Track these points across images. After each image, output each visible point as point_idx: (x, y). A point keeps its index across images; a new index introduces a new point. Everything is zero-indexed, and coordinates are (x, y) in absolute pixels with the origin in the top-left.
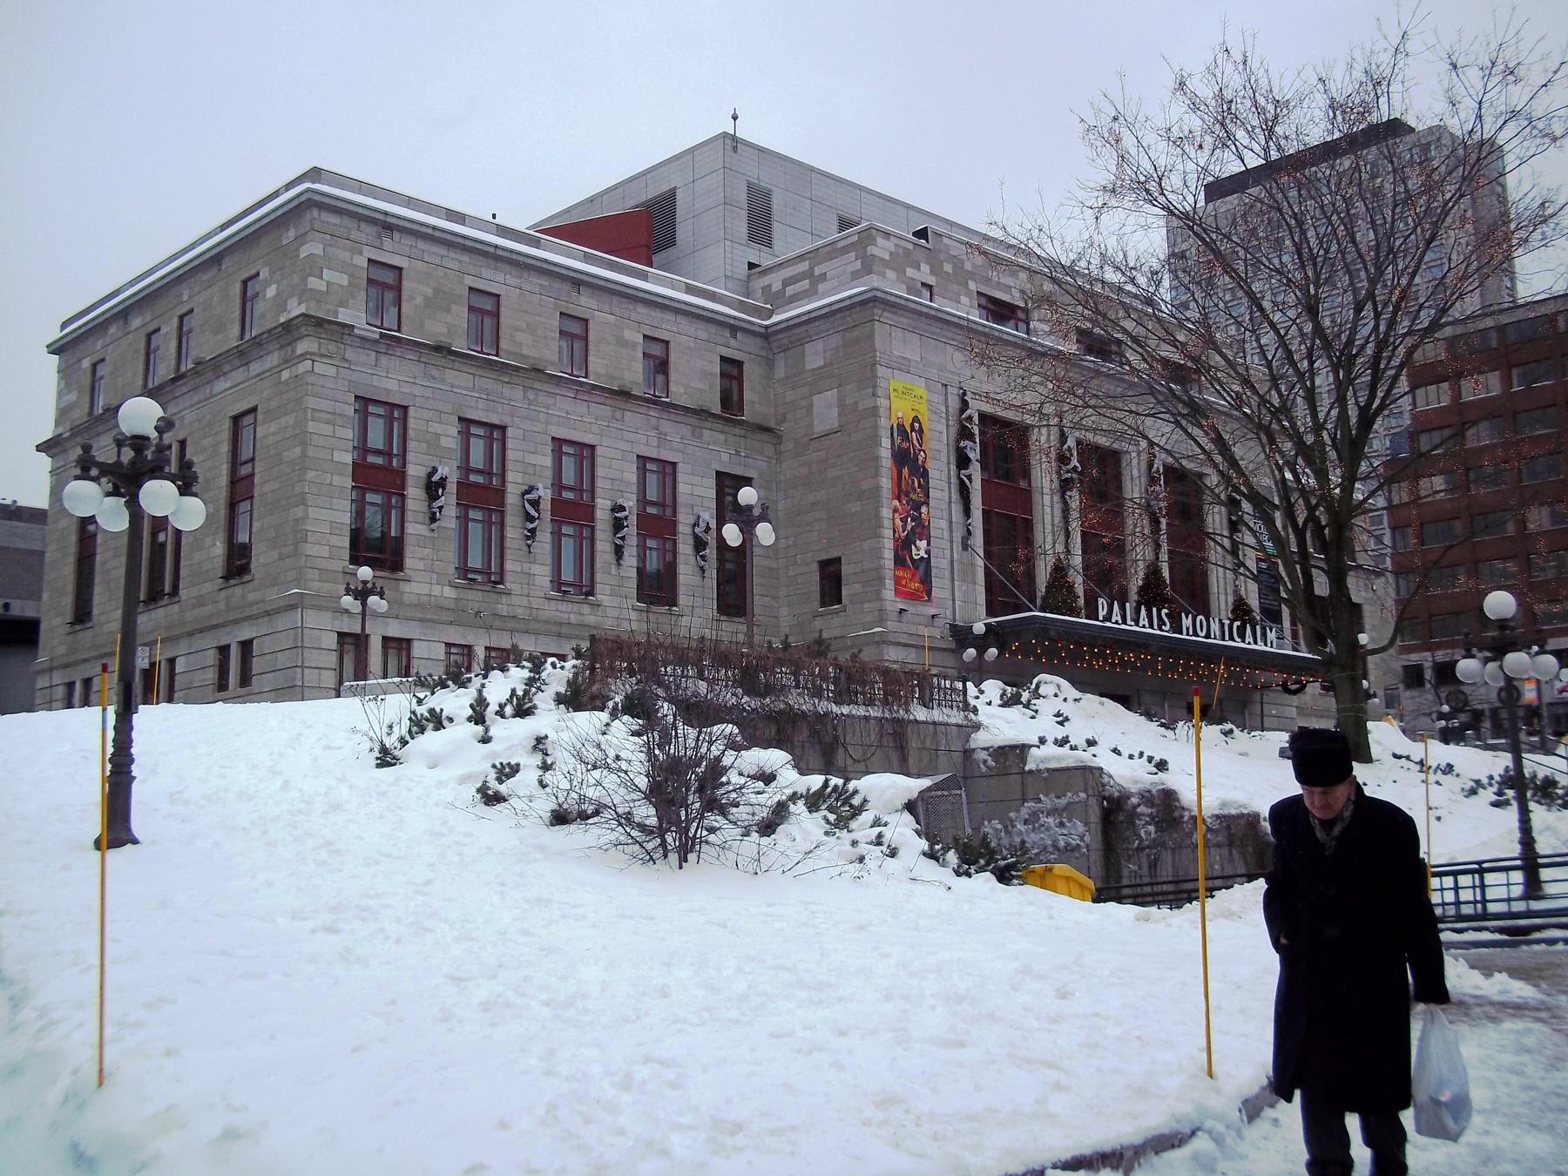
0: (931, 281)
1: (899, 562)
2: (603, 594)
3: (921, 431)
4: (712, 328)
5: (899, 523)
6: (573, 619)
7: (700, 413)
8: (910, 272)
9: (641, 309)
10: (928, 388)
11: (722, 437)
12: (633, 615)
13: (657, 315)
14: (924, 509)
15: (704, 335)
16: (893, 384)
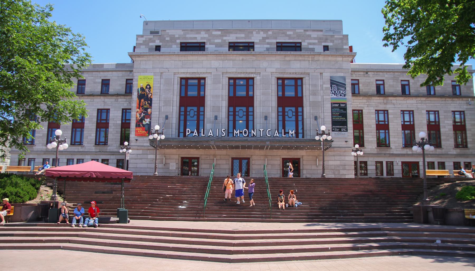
0: (160, 44)
1: (138, 125)
2: (85, 143)
3: (150, 88)
4: (124, 73)
5: (138, 115)
6: (76, 150)
7: (118, 95)
8: (151, 44)
9: (101, 73)
10: (155, 75)
11: (125, 100)
12: (94, 148)
13: (106, 73)
14: (149, 110)
15: (121, 75)
16: (140, 77)
